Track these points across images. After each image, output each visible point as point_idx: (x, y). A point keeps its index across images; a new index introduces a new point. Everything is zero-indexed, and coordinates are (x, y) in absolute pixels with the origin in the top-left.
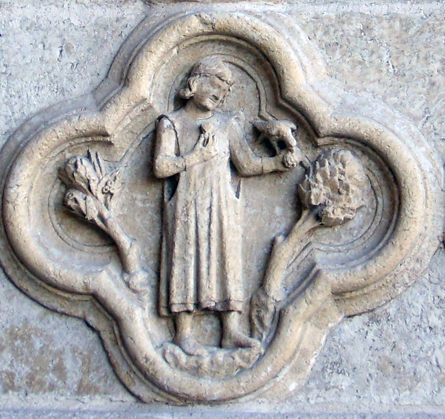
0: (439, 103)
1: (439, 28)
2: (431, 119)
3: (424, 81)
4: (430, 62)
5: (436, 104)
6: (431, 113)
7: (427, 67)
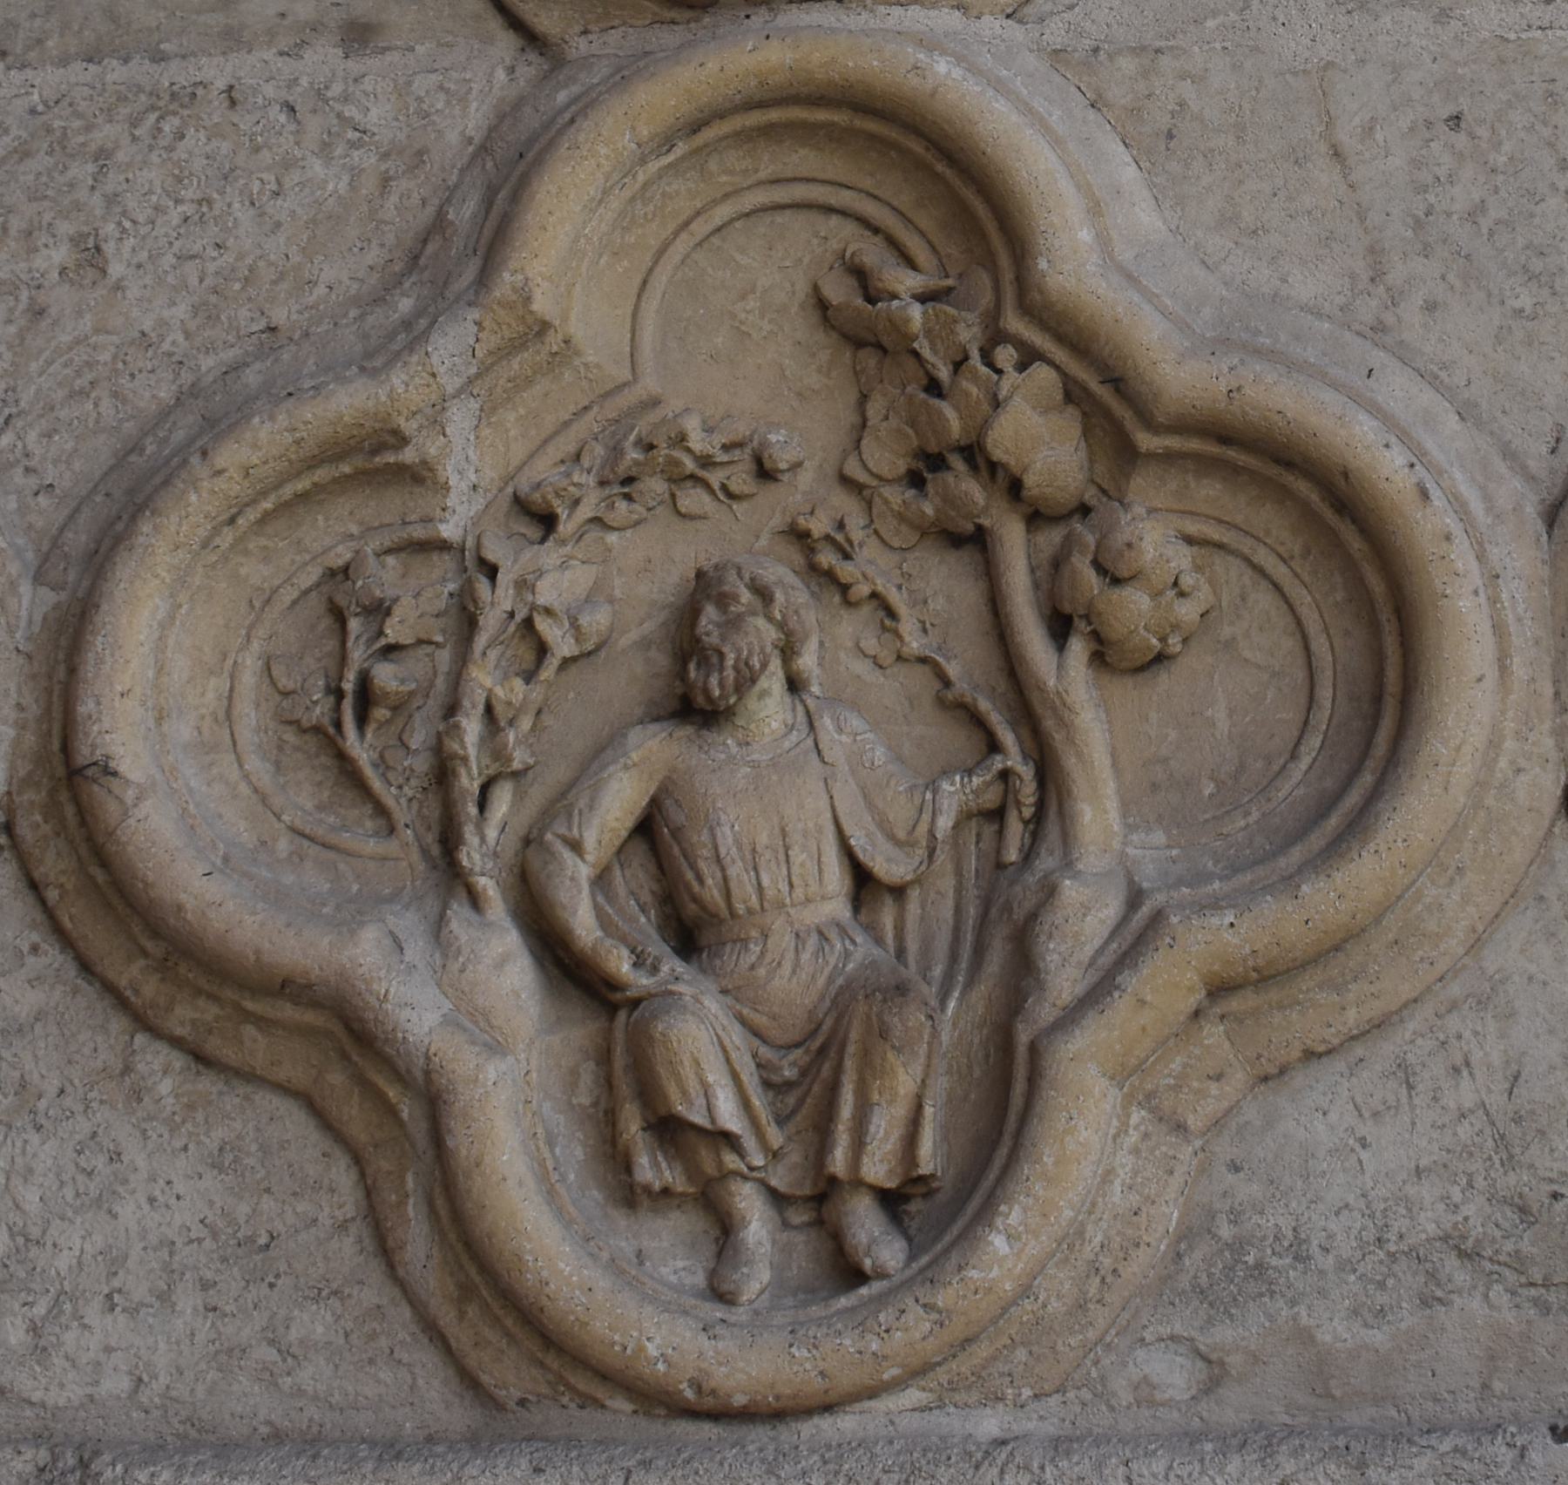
0: (51, 369)
1: (81, 139)
2: (20, 423)
3: (12, 304)
4: (39, 243)
5: (40, 375)
6: (23, 404)
7: (28, 260)
